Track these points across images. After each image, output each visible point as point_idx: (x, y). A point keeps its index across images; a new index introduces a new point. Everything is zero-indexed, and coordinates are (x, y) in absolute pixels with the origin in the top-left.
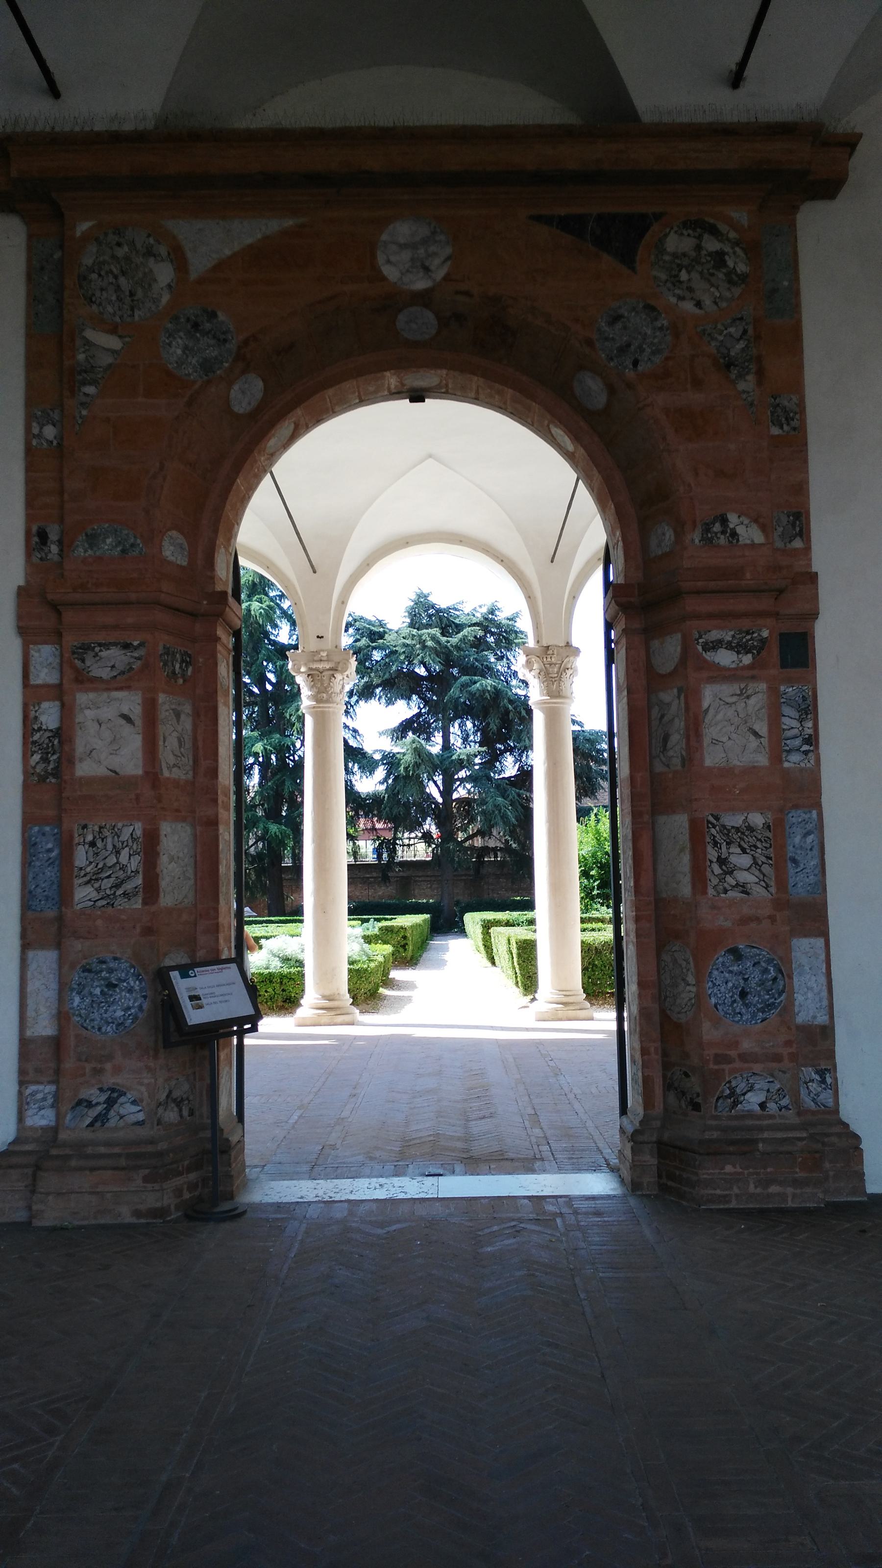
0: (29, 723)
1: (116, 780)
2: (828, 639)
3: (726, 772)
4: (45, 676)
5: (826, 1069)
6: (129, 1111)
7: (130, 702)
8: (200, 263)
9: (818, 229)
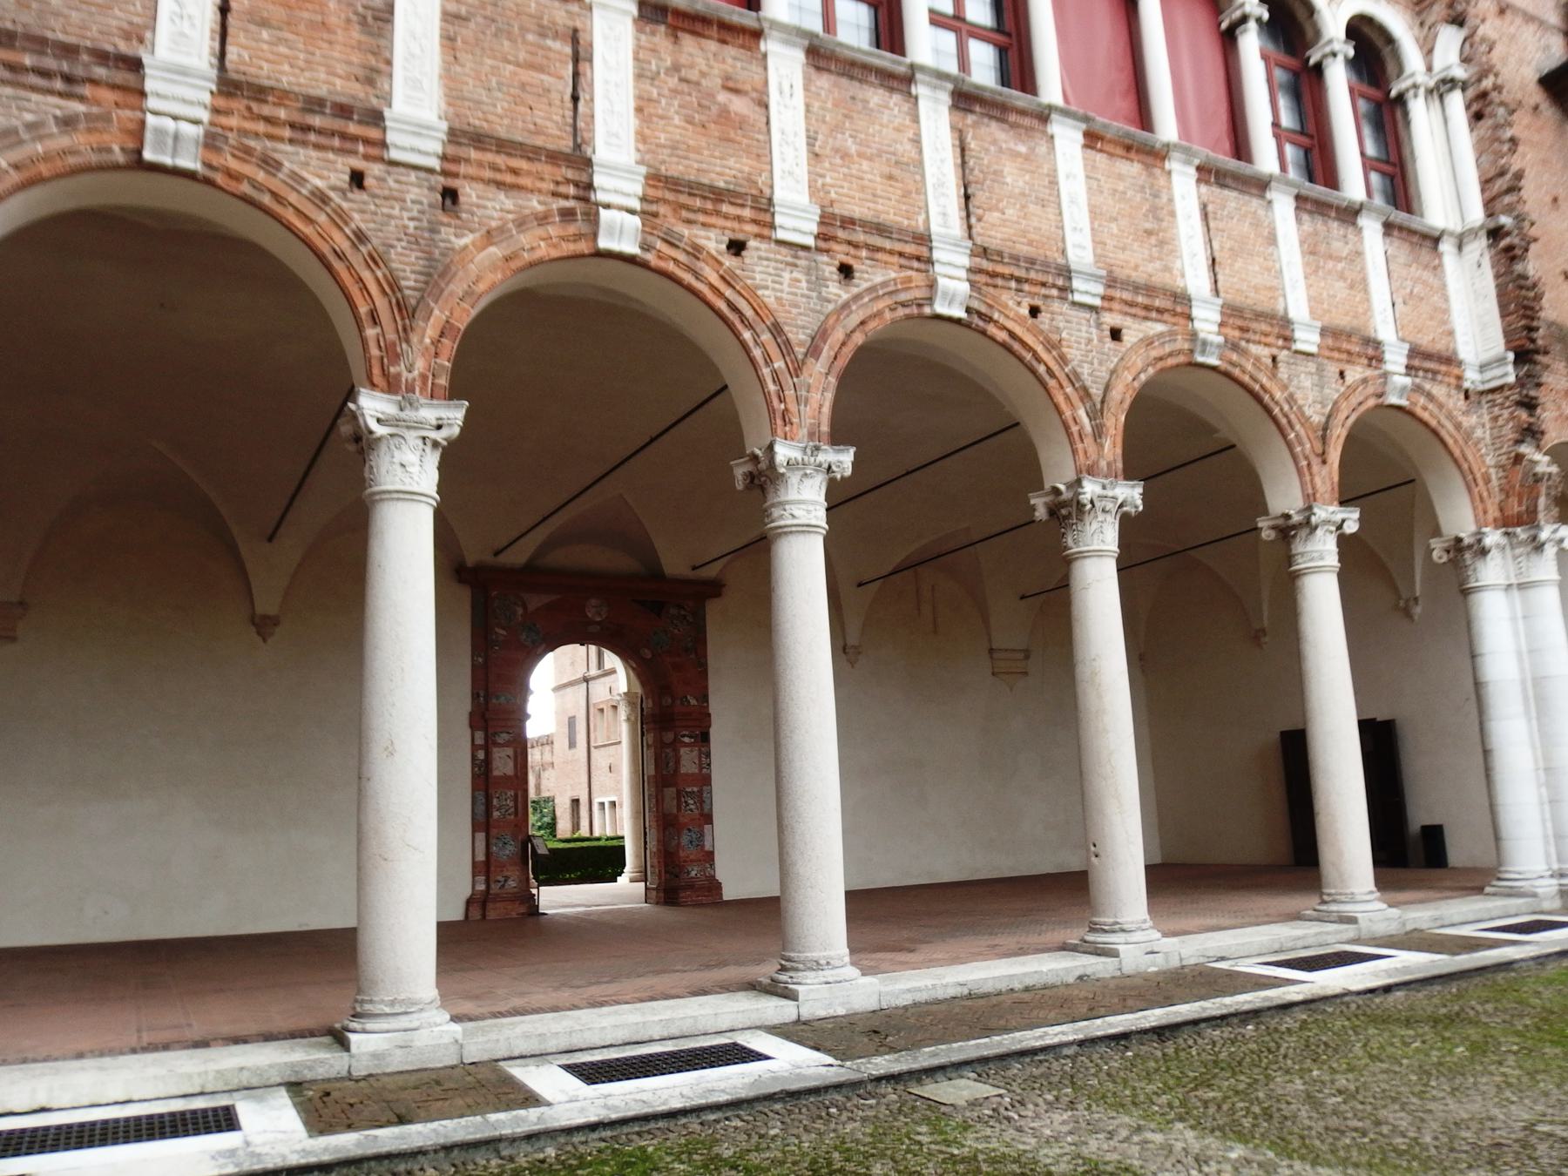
0: (474, 757)
1: (506, 777)
2: (715, 733)
3: (687, 775)
4: (480, 741)
5: (712, 865)
6: (512, 883)
7: (510, 751)
8: (531, 608)
9: (713, 609)
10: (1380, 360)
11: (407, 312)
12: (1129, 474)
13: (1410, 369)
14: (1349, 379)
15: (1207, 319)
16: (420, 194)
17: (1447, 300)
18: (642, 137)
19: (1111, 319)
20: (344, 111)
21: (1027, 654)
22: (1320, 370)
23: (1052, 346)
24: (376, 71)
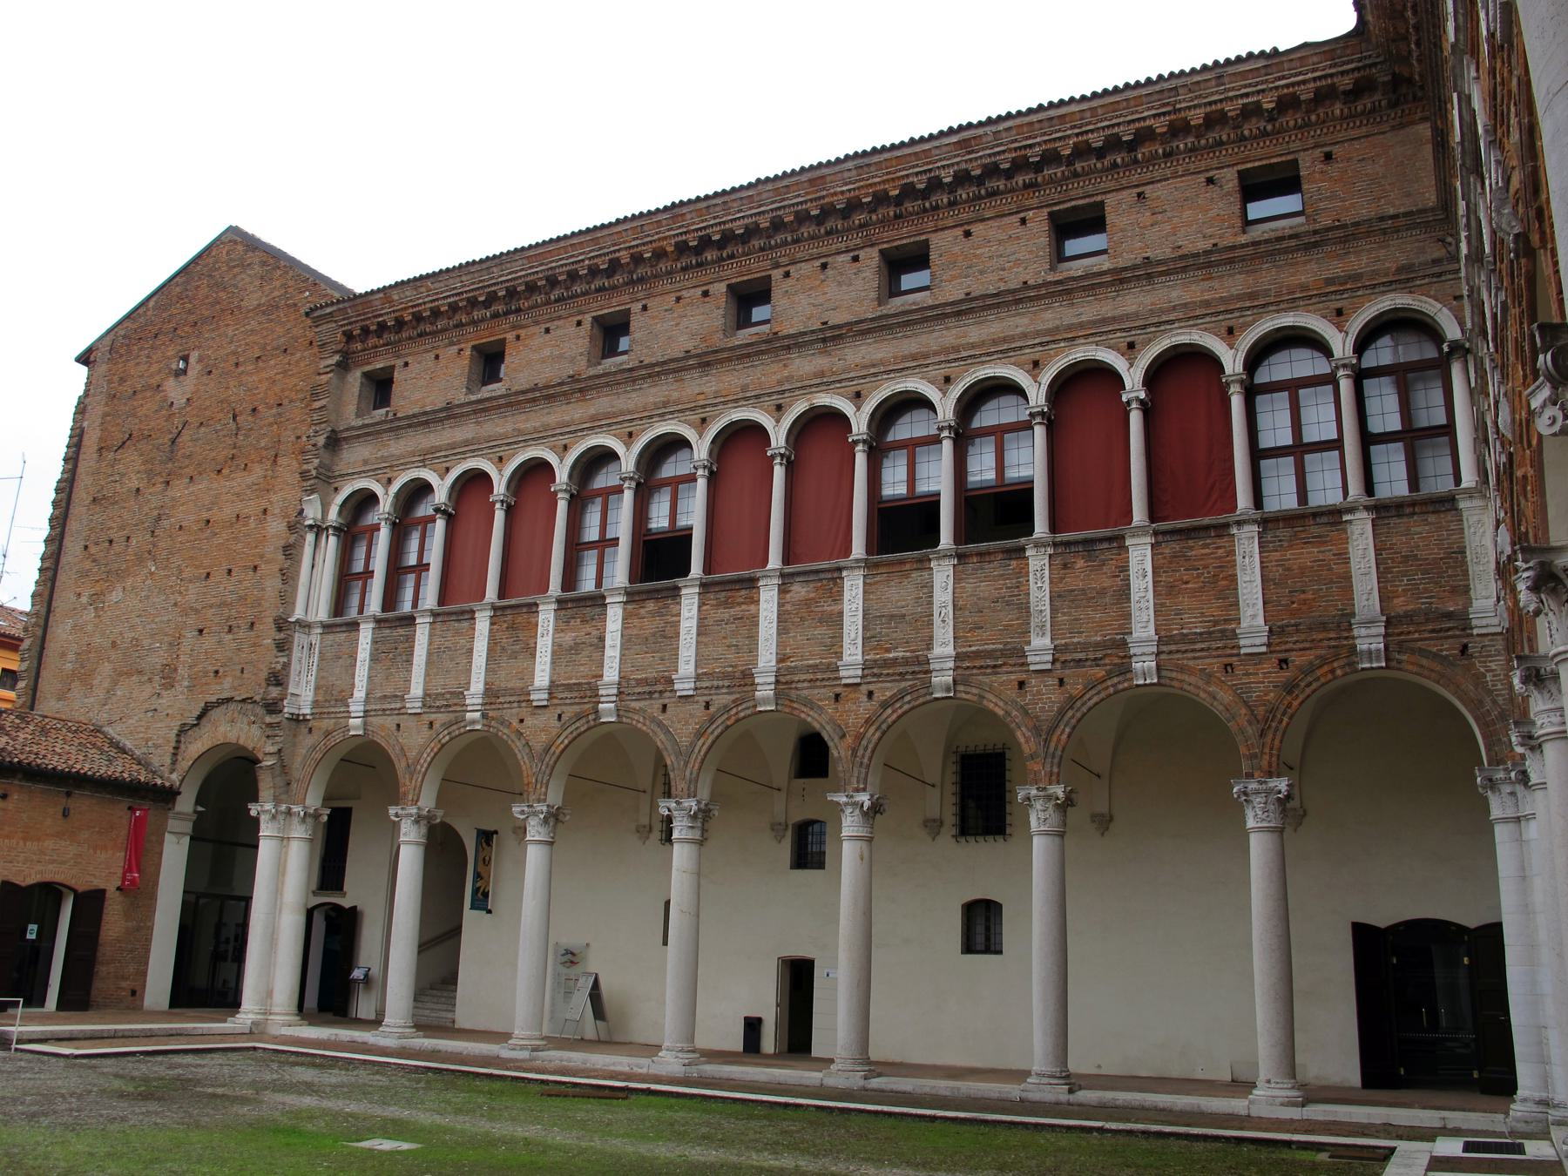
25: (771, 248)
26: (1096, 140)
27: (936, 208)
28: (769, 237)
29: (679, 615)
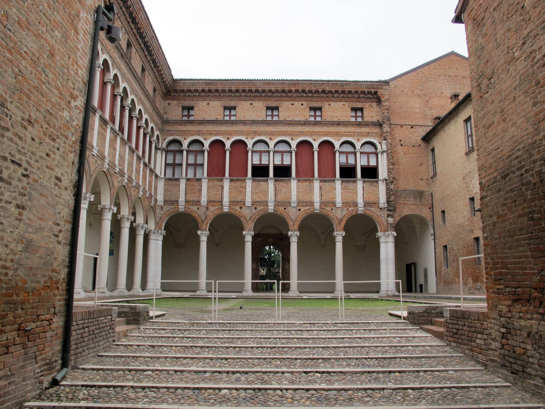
10: (357, 206)
11: (203, 222)
12: (299, 230)
13: (364, 206)
14: (349, 210)
15: (317, 206)
16: (204, 209)
17: (379, 192)
18: (229, 196)
19: (298, 208)
20: (197, 202)
21: (365, 246)
22: (343, 210)
23: (287, 213)
24: (200, 196)
25: (121, 9)
26: (157, 60)
27: (138, 42)
28: (124, 6)
29: (94, 122)
